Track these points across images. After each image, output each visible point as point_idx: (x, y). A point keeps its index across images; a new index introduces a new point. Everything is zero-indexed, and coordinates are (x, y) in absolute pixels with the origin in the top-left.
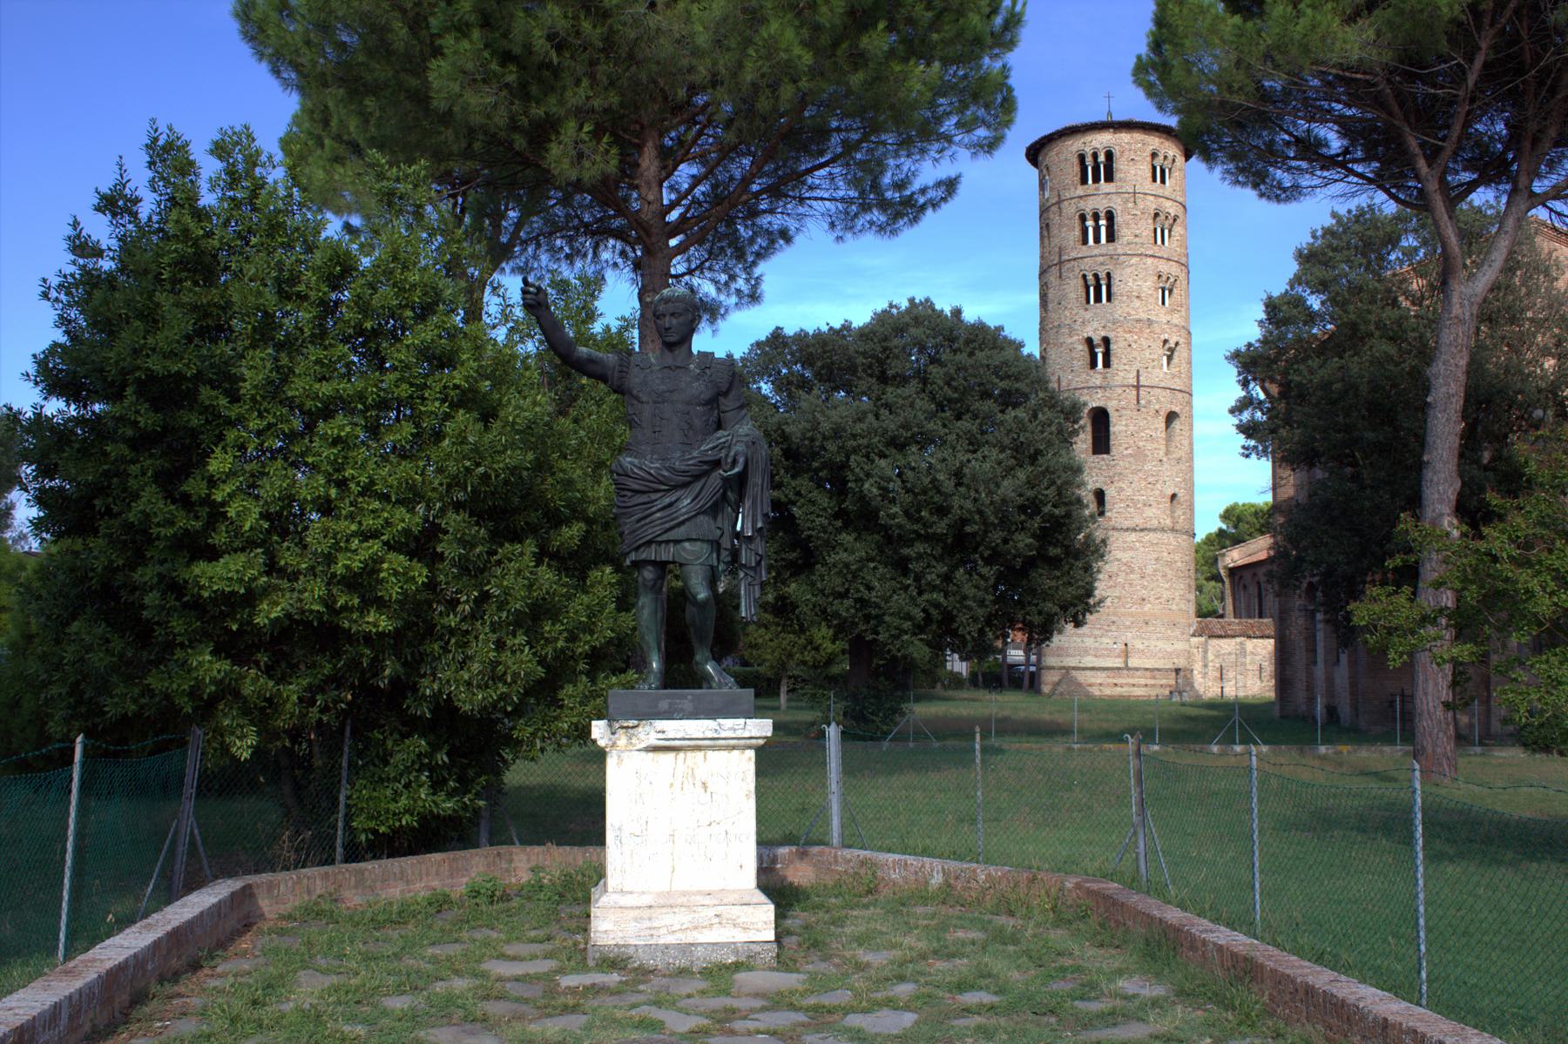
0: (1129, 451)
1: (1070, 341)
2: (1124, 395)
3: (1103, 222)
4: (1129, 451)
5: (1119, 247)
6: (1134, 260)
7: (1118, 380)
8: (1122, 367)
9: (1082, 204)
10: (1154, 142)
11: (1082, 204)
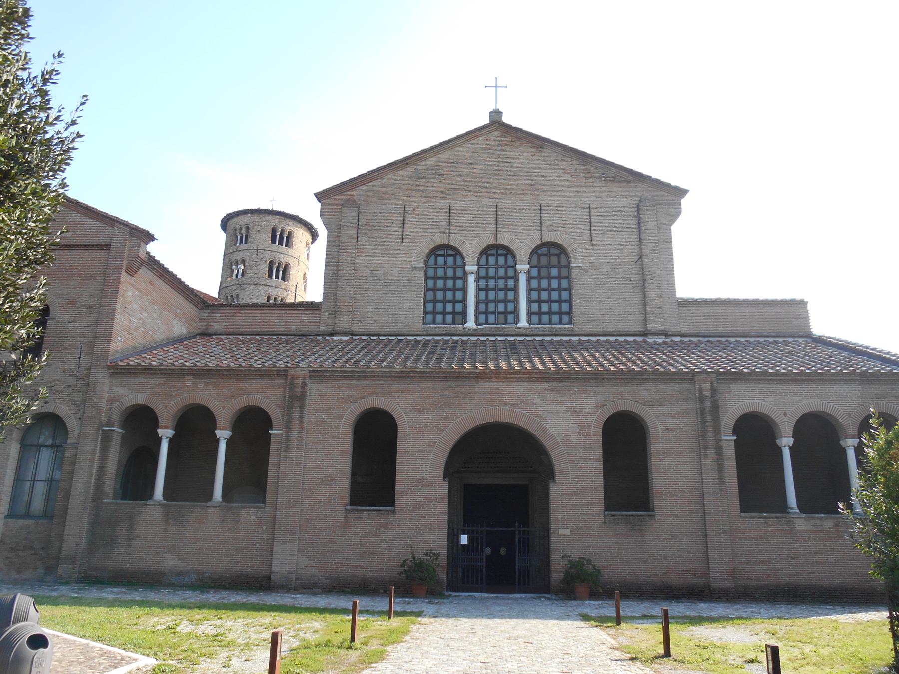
5: (245, 280)
6: (252, 287)
10: (275, 221)
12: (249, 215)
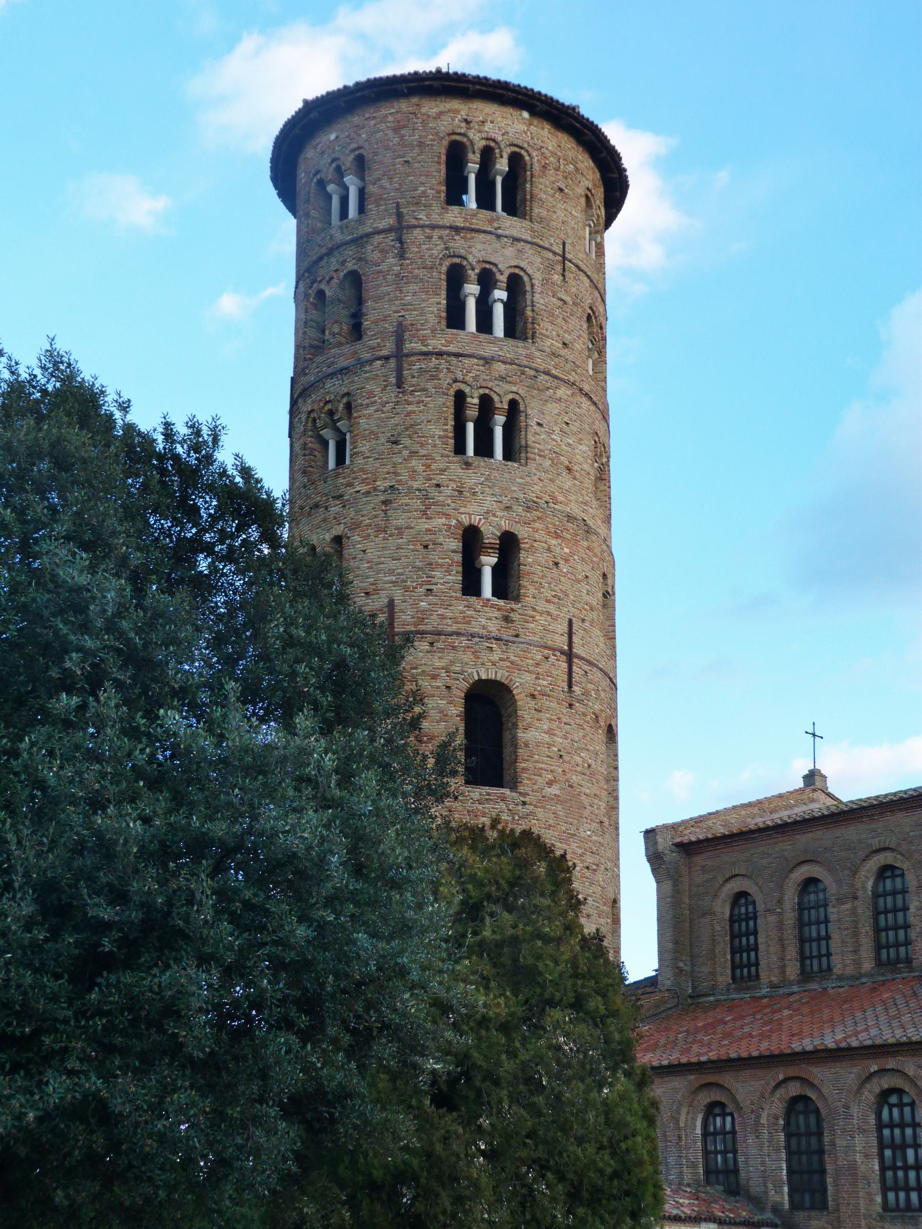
0: (554, 790)
1: (424, 525)
2: (545, 666)
3: (500, 294)
4: (554, 790)
7: (534, 630)
8: (542, 606)
9: (459, 244)
11: (459, 244)
12: (526, 115)
